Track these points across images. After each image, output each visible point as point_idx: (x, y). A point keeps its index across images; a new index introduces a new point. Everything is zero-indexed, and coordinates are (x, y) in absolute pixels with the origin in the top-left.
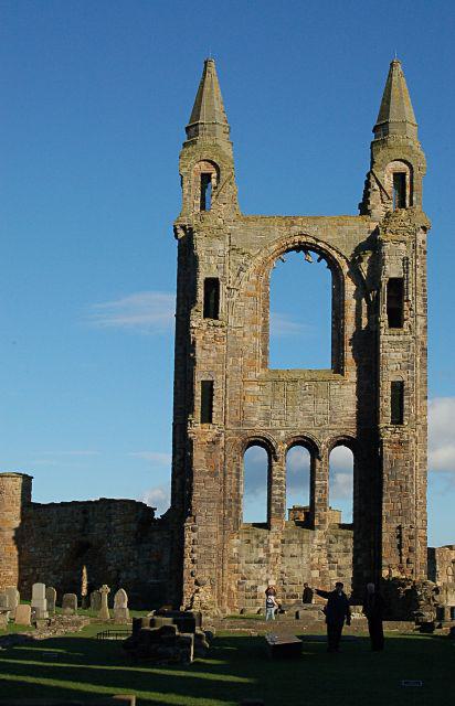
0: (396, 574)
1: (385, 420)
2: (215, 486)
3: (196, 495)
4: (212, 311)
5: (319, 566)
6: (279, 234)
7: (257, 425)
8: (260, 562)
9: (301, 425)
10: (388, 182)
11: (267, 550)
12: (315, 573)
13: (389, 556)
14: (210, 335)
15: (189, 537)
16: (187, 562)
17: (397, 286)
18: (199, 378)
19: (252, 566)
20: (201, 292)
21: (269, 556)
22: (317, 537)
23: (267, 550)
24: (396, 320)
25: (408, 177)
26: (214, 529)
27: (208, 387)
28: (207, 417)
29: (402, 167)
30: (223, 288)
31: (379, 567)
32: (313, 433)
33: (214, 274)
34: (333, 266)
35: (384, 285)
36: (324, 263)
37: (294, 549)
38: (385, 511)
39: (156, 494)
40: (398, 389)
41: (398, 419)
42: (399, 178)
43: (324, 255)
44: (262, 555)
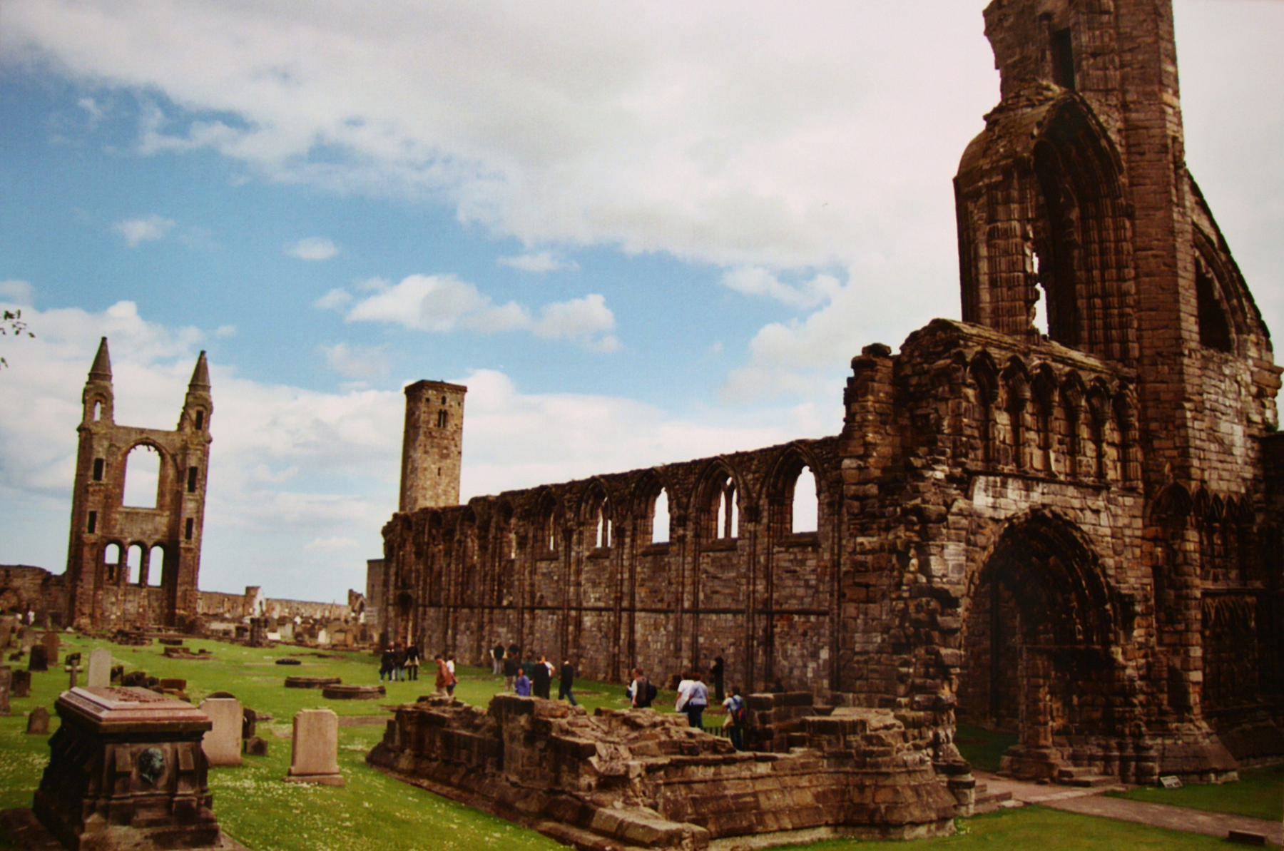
0: (182, 612)
1: (182, 538)
2: (92, 565)
3: (84, 569)
4: (98, 476)
5: (143, 607)
6: (134, 437)
7: (116, 533)
8: (113, 604)
9: (137, 537)
10: (194, 416)
11: (116, 597)
12: (141, 610)
13: (179, 603)
14: (97, 488)
15: (79, 590)
16: (77, 603)
17: (194, 471)
18: (90, 508)
19: (109, 606)
20: (93, 466)
21: (117, 600)
22: (144, 592)
23: (116, 597)
24: (192, 489)
25: (204, 415)
26: (92, 587)
27: (93, 515)
28: (92, 530)
29: (201, 408)
30: (105, 464)
31: (175, 608)
32: (145, 540)
33: (102, 456)
34: (162, 455)
35: (188, 471)
36: (157, 453)
37: (131, 597)
38: (179, 581)
39: (57, 565)
40: (190, 521)
41: (189, 536)
42: (200, 414)
43: (157, 448)
44: (113, 599)
